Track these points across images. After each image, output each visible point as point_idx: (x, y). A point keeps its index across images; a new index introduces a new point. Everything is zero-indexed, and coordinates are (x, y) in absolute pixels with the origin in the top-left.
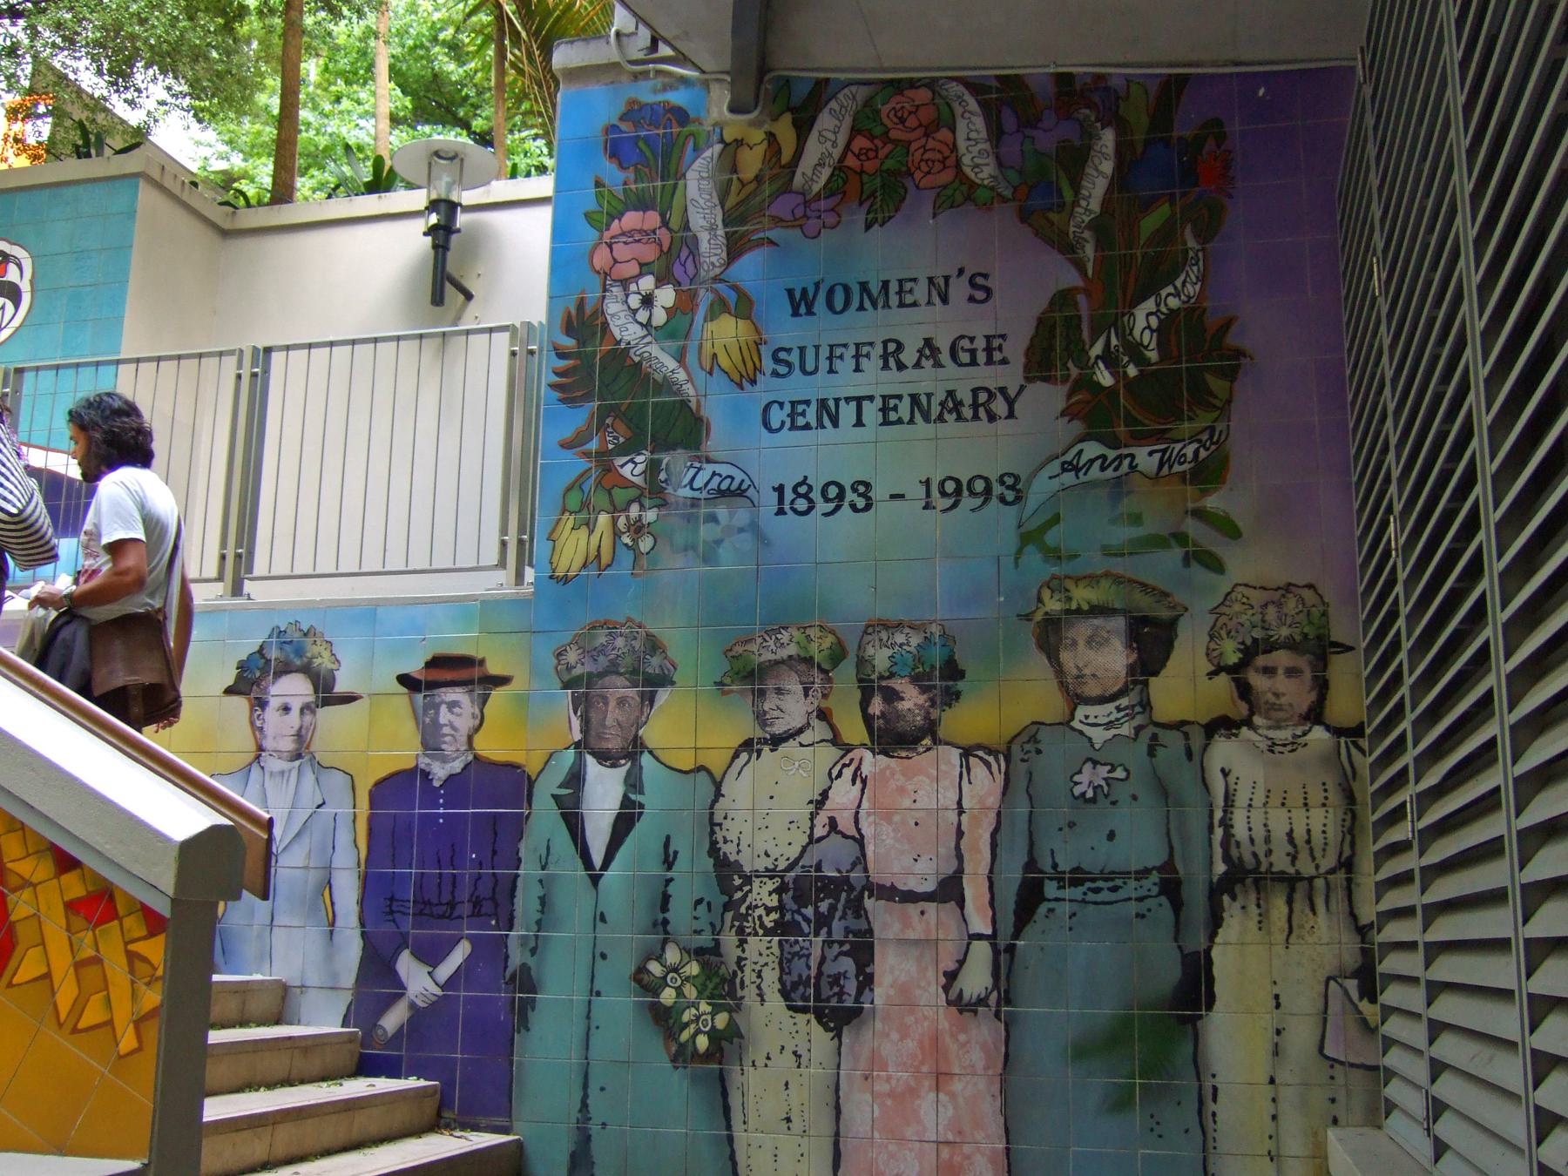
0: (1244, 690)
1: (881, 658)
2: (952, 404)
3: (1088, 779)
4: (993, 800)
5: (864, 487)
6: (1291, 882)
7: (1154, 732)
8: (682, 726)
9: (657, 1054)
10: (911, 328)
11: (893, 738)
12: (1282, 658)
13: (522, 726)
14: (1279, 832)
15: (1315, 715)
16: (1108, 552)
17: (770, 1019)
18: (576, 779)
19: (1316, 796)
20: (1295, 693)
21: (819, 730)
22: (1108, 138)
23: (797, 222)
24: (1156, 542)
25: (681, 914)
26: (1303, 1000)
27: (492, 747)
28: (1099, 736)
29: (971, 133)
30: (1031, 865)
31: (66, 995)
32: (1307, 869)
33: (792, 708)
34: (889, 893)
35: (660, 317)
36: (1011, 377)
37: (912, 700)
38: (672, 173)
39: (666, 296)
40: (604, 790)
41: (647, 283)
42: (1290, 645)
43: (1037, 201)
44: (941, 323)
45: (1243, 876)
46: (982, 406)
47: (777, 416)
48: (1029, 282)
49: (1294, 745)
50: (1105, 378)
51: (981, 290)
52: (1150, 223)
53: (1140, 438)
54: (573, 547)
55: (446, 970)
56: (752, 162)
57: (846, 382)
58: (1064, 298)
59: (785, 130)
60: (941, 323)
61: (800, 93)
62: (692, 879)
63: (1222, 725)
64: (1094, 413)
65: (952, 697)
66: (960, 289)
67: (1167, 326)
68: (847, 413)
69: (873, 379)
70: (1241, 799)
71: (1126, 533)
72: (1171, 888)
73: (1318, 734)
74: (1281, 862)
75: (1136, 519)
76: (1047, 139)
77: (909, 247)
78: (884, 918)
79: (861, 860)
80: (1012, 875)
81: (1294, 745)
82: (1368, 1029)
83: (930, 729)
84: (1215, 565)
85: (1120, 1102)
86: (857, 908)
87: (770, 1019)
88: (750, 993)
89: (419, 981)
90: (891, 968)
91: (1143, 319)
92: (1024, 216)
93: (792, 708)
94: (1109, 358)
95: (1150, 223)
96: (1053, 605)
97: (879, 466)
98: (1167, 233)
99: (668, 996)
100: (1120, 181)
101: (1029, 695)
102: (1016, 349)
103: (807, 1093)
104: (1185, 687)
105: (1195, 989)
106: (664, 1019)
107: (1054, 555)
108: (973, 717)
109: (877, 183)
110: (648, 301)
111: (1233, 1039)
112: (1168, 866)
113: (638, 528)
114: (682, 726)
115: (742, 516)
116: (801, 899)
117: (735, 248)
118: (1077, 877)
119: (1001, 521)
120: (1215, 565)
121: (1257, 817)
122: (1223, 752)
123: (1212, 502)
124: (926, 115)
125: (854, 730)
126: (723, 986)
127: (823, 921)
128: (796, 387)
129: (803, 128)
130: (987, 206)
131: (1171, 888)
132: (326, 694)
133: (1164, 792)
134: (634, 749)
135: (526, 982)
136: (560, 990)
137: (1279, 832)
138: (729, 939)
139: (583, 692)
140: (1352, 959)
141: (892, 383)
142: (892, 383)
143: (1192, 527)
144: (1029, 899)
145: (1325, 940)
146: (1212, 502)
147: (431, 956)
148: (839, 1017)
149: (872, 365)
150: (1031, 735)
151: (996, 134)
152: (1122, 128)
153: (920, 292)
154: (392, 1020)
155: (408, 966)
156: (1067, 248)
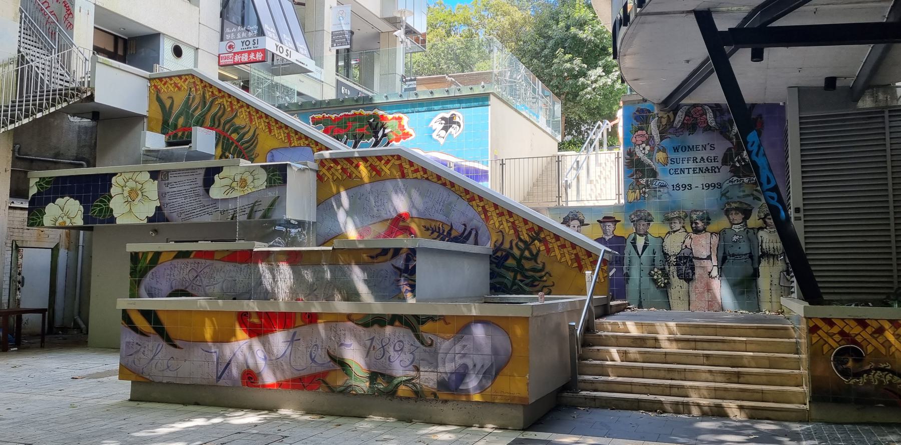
0: (765, 222)
1: (694, 217)
2: (707, 170)
3: (735, 238)
5: (690, 185)
6: (774, 256)
7: (747, 230)
8: (656, 229)
11: (697, 231)
14: (771, 246)
17: (676, 281)
18: (635, 239)
21: (683, 230)
24: (748, 195)
25: (657, 262)
26: (776, 276)
27: (617, 233)
28: (737, 230)
29: (710, 117)
30: (724, 253)
33: (677, 226)
35: (647, 152)
36: (719, 164)
37: (700, 225)
39: (648, 148)
40: (640, 242)
41: (644, 145)
43: (723, 130)
44: (705, 154)
45: (765, 255)
46: (713, 170)
47: (672, 172)
48: (722, 147)
50: (738, 165)
51: (713, 147)
53: (745, 176)
54: (632, 196)
56: (664, 121)
57: (685, 165)
58: (730, 149)
60: (705, 154)
62: (659, 256)
63: (761, 228)
64: (735, 171)
65: (708, 224)
66: (708, 147)
68: (686, 171)
69: (691, 165)
71: (742, 194)
72: (751, 256)
74: (772, 252)
75: (744, 191)
77: (698, 139)
79: (692, 253)
80: (721, 255)
83: (704, 229)
85: (742, 293)
87: (676, 281)
90: (698, 271)
92: (721, 133)
93: (677, 226)
94: (739, 161)
97: (692, 182)
99: (655, 277)
101: (722, 223)
102: (720, 159)
105: (756, 274)
106: (655, 281)
107: (728, 198)
108: (714, 227)
109: (691, 126)
110: (644, 149)
111: (764, 283)
113: (644, 193)
114: (656, 229)
115: (666, 190)
116: (681, 260)
117: (662, 139)
118: (733, 255)
119: (717, 192)
122: (761, 233)
124: (701, 112)
125: (689, 229)
126: (666, 275)
127: (685, 263)
128: (675, 166)
129: (675, 115)
130: (713, 131)
131: (751, 256)
132: (582, 223)
133: (749, 240)
135: (627, 275)
136: (635, 274)
137: (771, 246)
138: (667, 267)
143: (755, 193)
148: (689, 279)
150: (724, 230)
151: (715, 116)
153: (700, 148)
156: (730, 139)
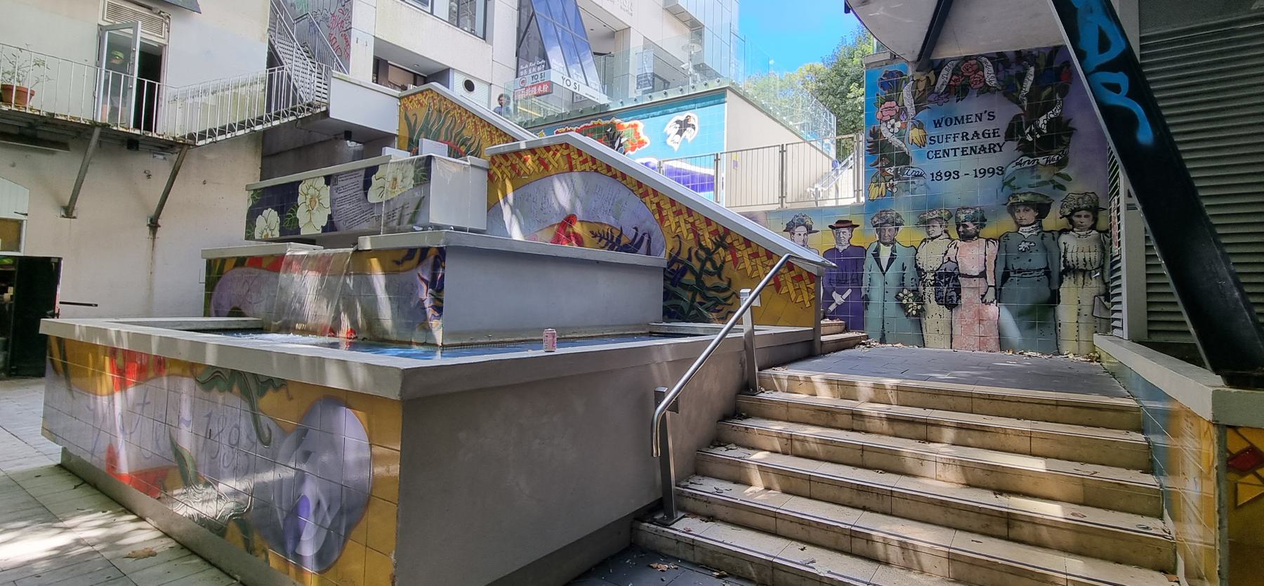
0: (1071, 222)
1: (962, 217)
2: (983, 149)
3: (1023, 245)
4: (995, 252)
5: (957, 173)
6: (1084, 272)
7: (1043, 233)
8: (907, 235)
9: (902, 315)
10: (970, 129)
11: (966, 237)
12: (1083, 213)
13: (864, 237)
14: (1081, 259)
15: (1093, 227)
16: (1030, 186)
17: (933, 307)
18: (877, 250)
19: (1093, 248)
20: (1087, 222)
21: (945, 235)
22: (1032, 69)
23: (936, 101)
24: (1045, 183)
25: (908, 281)
26: (1087, 301)
27: (854, 243)
28: (1026, 235)
29: (989, 73)
30: (1006, 268)
31: (793, 296)
32: (1089, 267)
33: (937, 230)
34: (966, 276)
35: (896, 130)
36: (1001, 140)
37: (971, 227)
38: (899, 90)
39: (898, 124)
40: (885, 253)
41: (893, 121)
42: (1086, 209)
43: (1009, 90)
44: (979, 127)
45: (1070, 270)
46: (992, 149)
47: (931, 155)
48: (1006, 112)
49: (1086, 235)
50: (1030, 138)
51: (992, 116)
52: (1045, 93)
53: (1040, 155)
54: (875, 192)
55: (845, 296)
56: (922, 86)
57: (951, 144)
58: (1017, 117)
59: (932, 75)
60: (979, 127)
61: (936, 64)
62: (910, 273)
63: (1065, 231)
64: (1026, 149)
65: (983, 226)
66: (985, 117)
67: (1050, 123)
68: (952, 153)
69: (960, 143)
70: (1070, 250)
71: (1036, 181)
72: (1048, 273)
73: (1094, 232)
74: (1081, 266)
75: (1039, 177)
76: (1013, 72)
77: (972, 105)
78: (964, 282)
79: (957, 268)
80: (1001, 270)
81: (1086, 235)
82: (1107, 309)
83: (977, 234)
84: (1063, 188)
85: (1032, 326)
86: (956, 279)
87: (933, 307)
88: (927, 301)
89: (838, 299)
90: (965, 294)
91: (1042, 122)
92: (1005, 95)
93: (937, 230)
94: (1031, 133)
95: (1045, 93)
96: (1012, 201)
98: (1051, 96)
99: (905, 302)
100: (1035, 82)
101: (1004, 224)
102: (1002, 133)
103: (943, 325)
104: (1053, 221)
105: (1055, 298)
106: (905, 307)
107: (1013, 188)
108: (990, 230)
109: (959, 90)
110: (893, 126)
111: (1066, 312)
112: (1047, 268)
113: (892, 186)
114: (907, 235)
115: (922, 181)
116: (941, 278)
117: (917, 110)
118: (1020, 271)
119: (996, 180)
120: (1063, 188)
121: (1074, 255)
122: (1064, 238)
123: (1062, 171)
124: (975, 67)
125: (954, 235)
126: (920, 299)
127: (946, 283)
128: (937, 147)
129: (937, 75)
130: (994, 92)
131: (1048, 273)
132: (810, 230)
133: (1045, 249)
134: (893, 242)
135: (867, 298)
137: (1081, 259)
138: (921, 288)
139: (879, 227)
140: (1102, 290)
141: (965, 144)
142: (965, 144)
143: (1057, 179)
144: (1005, 277)
145: (1094, 286)
146: (1062, 171)
147: (841, 293)
148: (951, 306)
149: (959, 139)
150: (1006, 235)
151: (996, 71)
152: (1037, 66)
153: (973, 118)
154: (832, 308)
155: (835, 295)
156: (1018, 103)
